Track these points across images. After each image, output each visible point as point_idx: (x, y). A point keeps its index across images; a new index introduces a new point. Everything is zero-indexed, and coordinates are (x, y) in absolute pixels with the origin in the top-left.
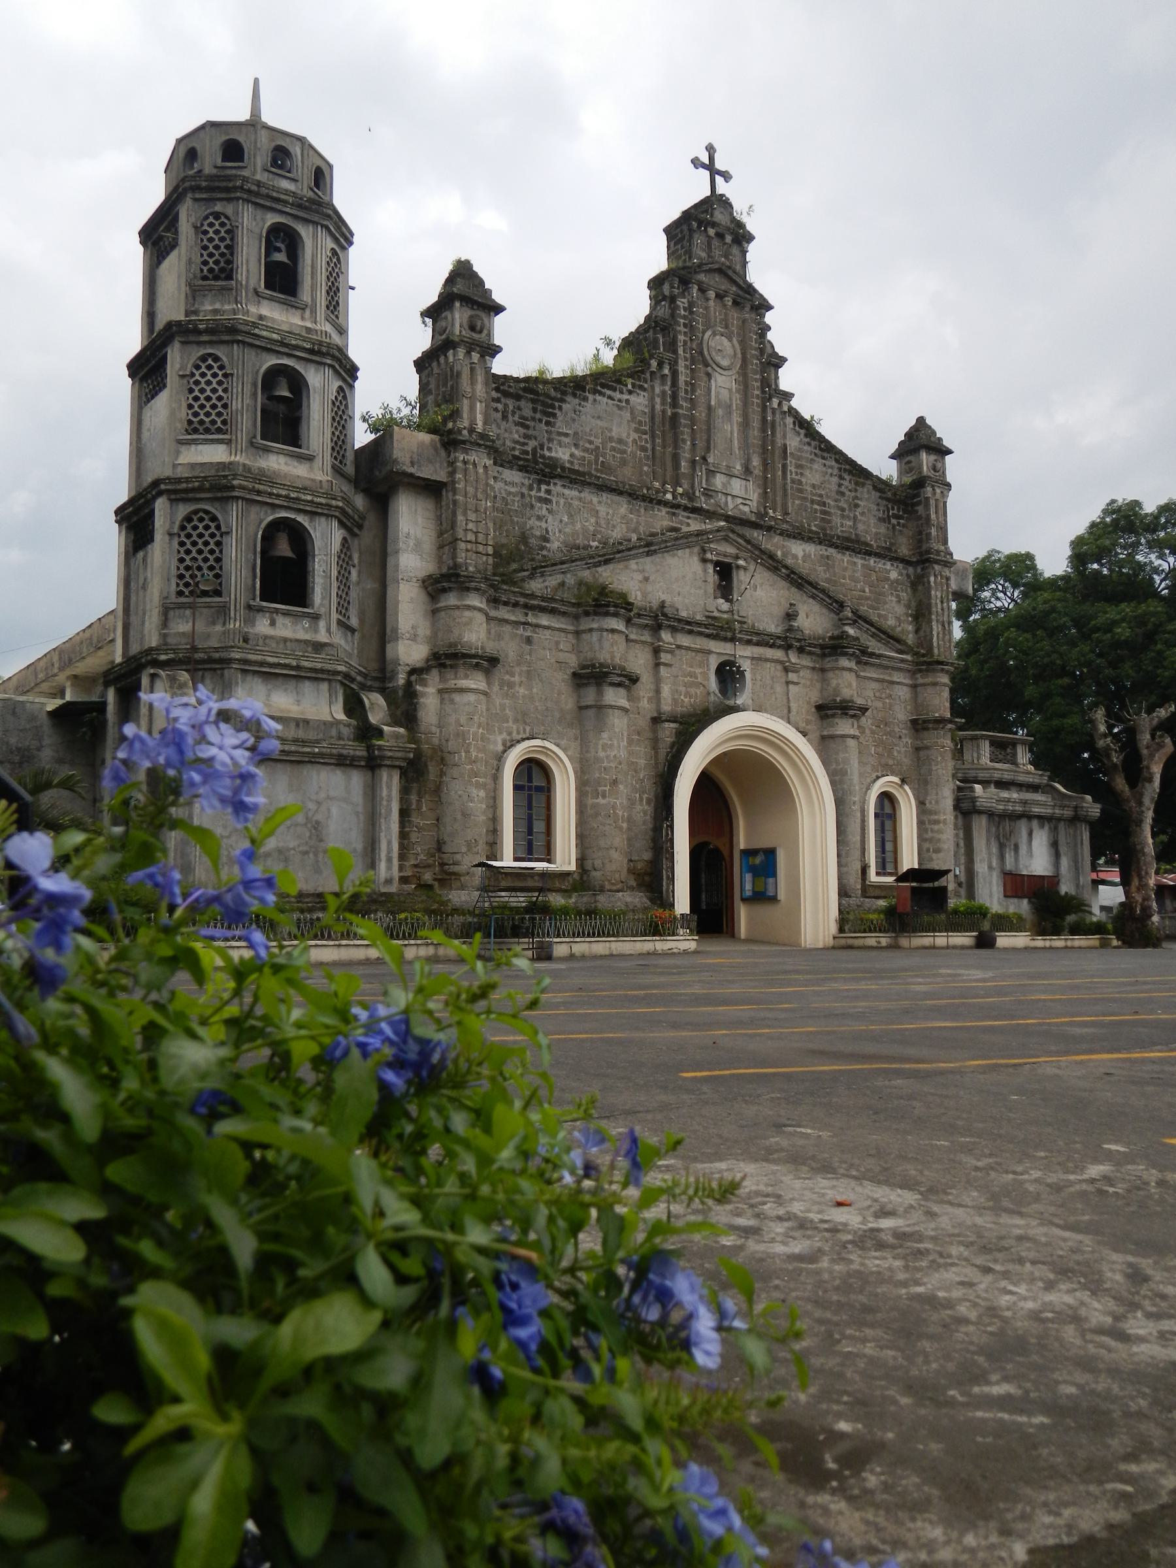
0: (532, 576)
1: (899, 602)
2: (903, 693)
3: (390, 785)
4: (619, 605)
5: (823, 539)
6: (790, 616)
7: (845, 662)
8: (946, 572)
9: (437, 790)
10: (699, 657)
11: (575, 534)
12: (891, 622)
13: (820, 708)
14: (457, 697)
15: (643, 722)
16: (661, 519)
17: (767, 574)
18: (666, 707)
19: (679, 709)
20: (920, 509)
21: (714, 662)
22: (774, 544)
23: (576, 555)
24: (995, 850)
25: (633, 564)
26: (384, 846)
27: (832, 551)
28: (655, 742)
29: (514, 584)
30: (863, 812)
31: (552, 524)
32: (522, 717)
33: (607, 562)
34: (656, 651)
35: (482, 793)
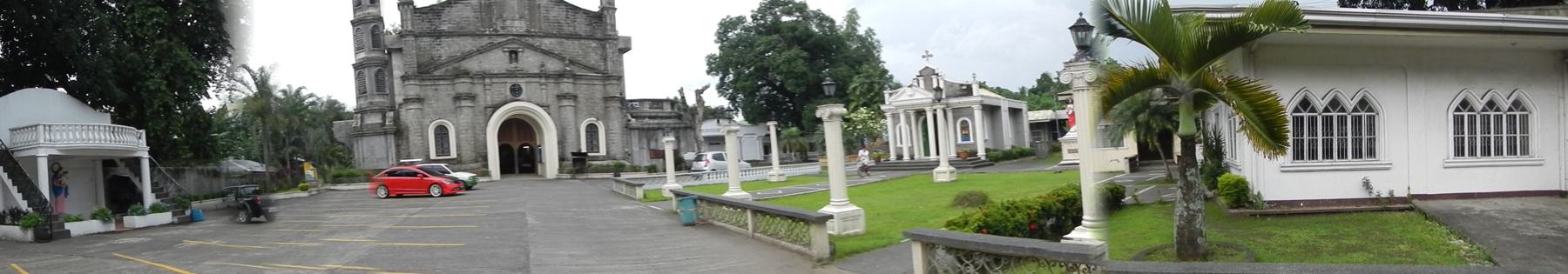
0: (436, 69)
1: (597, 54)
2: (599, 88)
3: (391, 139)
4: (466, 74)
5: (560, 36)
6: (543, 66)
7: (565, 80)
8: (615, 42)
9: (407, 138)
10: (503, 85)
11: (451, 53)
12: (593, 62)
13: (558, 96)
14: (410, 111)
15: (483, 109)
16: (485, 41)
17: (534, 52)
18: (489, 103)
19: (495, 103)
20: (604, 19)
21: (509, 86)
22: (536, 42)
23: (448, 62)
24: (645, 141)
25: (475, 58)
26: (390, 155)
27: (563, 40)
28: (486, 114)
29: (428, 73)
30: (578, 131)
31: (442, 51)
32: (436, 113)
33: (464, 59)
34: (485, 85)
35: (420, 138)
